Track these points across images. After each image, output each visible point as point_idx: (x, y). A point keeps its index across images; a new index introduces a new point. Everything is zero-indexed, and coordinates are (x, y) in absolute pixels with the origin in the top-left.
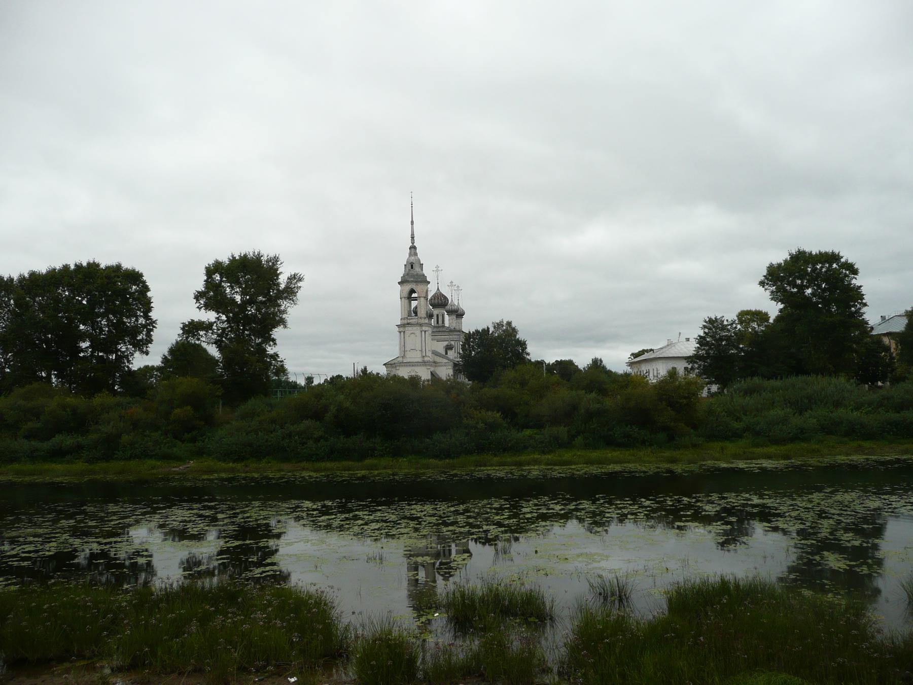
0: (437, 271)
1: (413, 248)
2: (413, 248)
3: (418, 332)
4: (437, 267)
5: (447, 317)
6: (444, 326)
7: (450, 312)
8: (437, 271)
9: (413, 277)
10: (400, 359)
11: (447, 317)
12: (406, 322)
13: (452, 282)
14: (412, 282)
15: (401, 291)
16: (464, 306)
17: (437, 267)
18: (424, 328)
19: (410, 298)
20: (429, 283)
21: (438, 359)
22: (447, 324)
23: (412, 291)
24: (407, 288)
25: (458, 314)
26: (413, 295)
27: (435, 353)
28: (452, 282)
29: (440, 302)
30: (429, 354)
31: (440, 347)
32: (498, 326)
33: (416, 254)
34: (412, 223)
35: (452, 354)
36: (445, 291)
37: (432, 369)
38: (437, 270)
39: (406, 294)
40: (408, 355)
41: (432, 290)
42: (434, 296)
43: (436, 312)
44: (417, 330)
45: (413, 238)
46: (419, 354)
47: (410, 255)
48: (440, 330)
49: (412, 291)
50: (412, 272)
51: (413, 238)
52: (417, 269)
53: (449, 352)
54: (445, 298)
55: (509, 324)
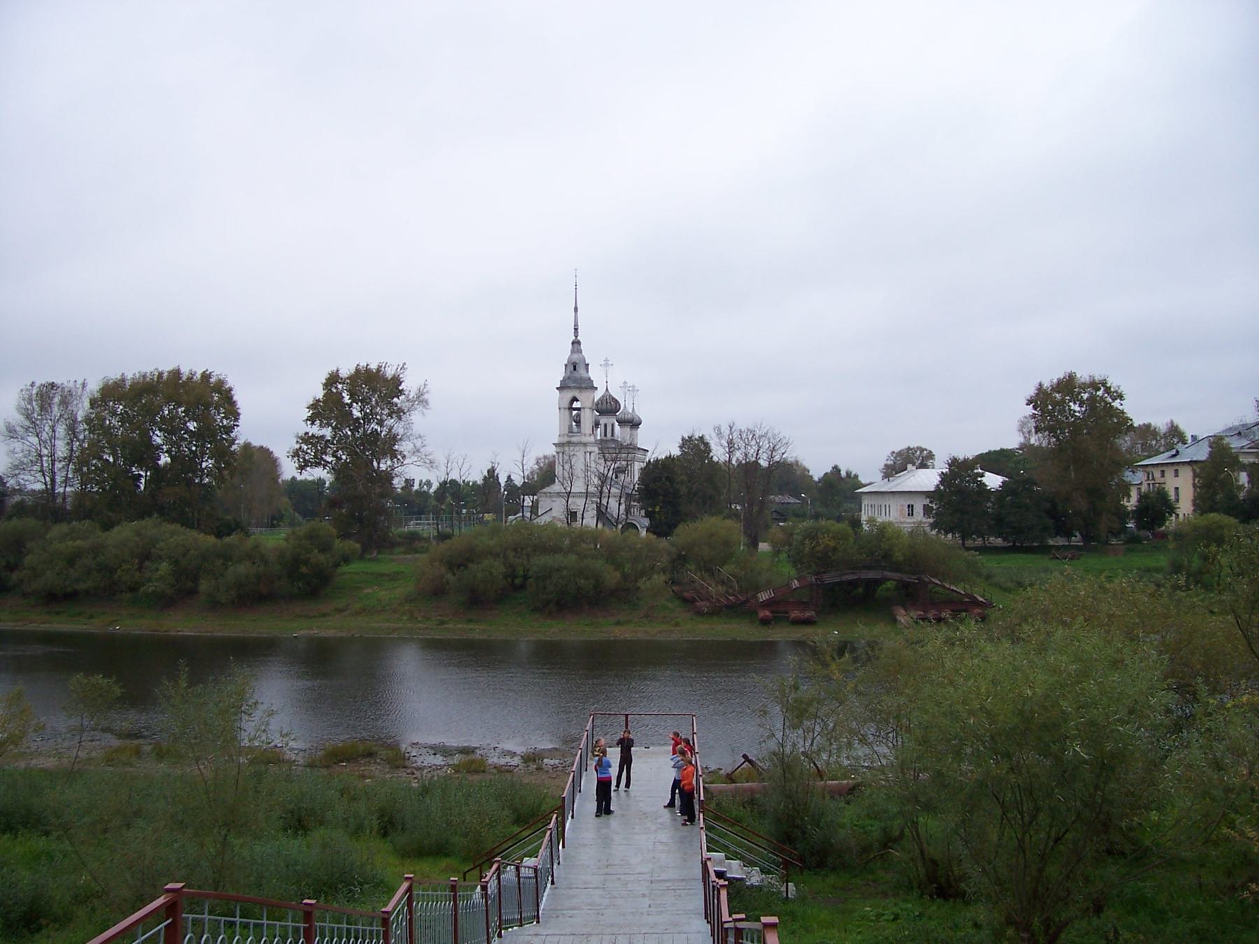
0: (606, 365)
1: (576, 343)
2: (576, 343)
4: (606, 360)
5: (617, 427)
7: (622, 423)
8: (606, 365)
11: (617, 427)
12: (566, 439)
15: (561, 399)
16: (641, 413)
17: (606, 360)
18: (589, 449)
19: (571, 409)
24: (569, 395)
25: (634, 424)
26: (576, 405)
29: (608, 407)
34: (576, 309)
39: (566, 404)
41: (598, 395)
42: (601, 400)
43: (603, 420)
47: (573, 352)
49: (575, 399)
50: (576, 374)
51: (576, 329)
52: (581, 372)
54: (616, 402)
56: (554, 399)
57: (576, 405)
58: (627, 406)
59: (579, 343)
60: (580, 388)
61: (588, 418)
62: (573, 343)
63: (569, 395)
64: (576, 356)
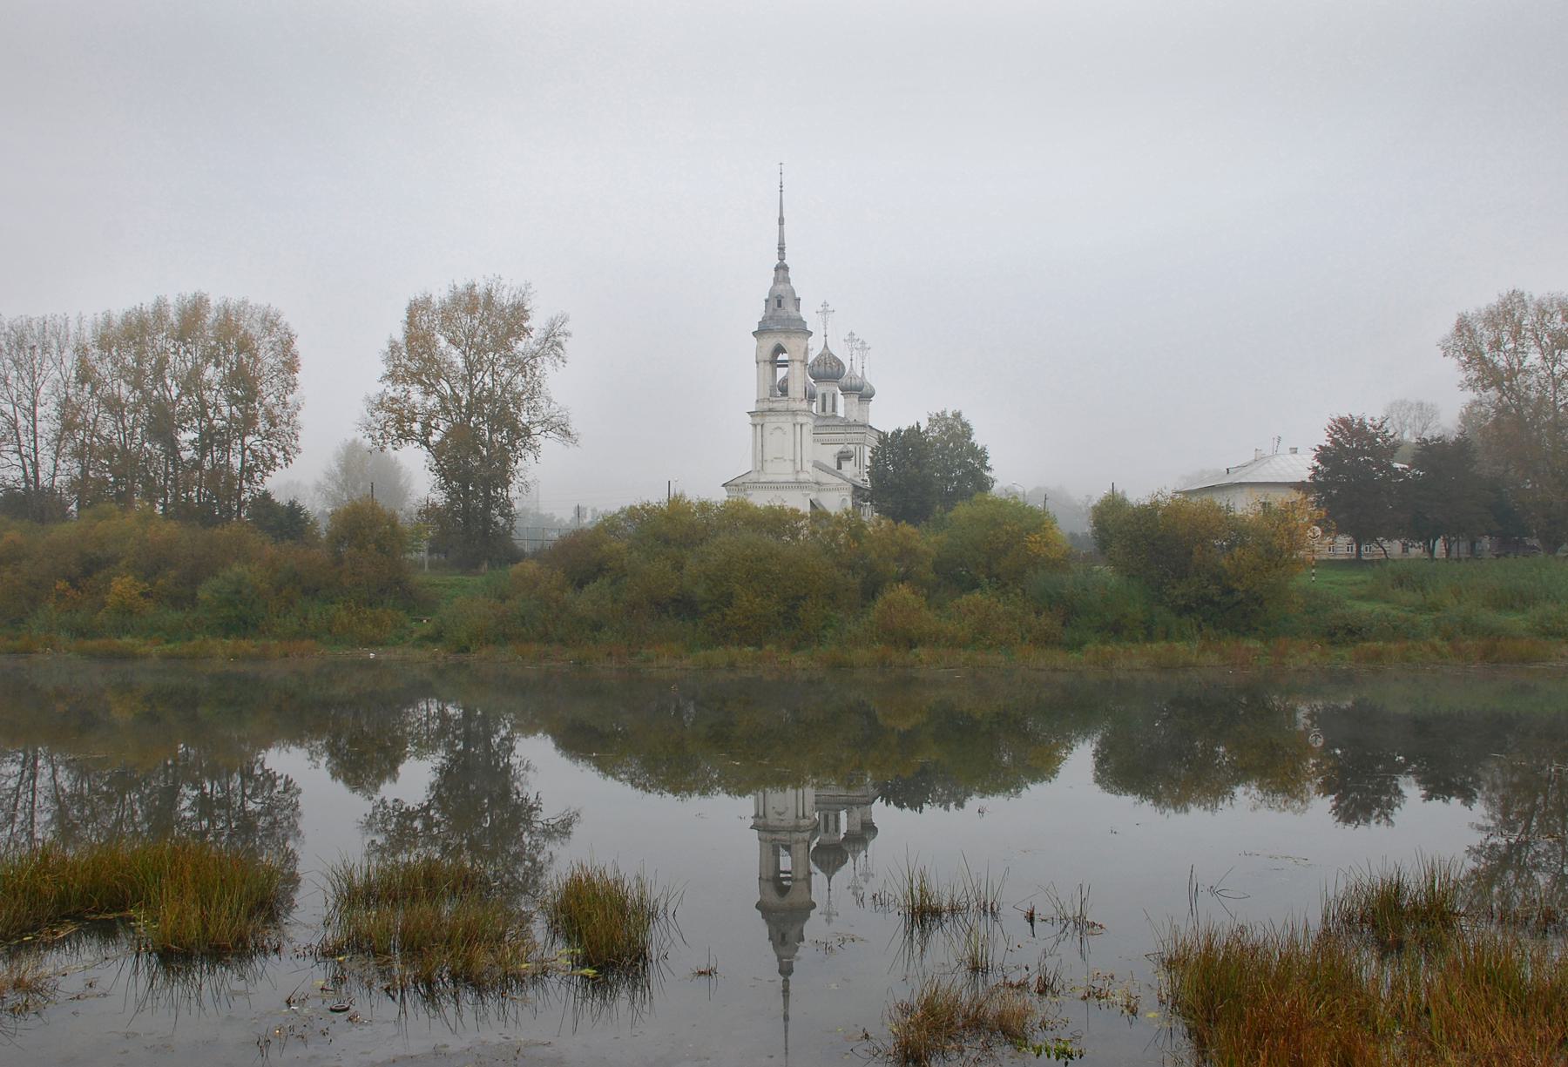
0: (825, 312)
1: (782, 269)
2: (782, 269)
3: (788, 427)
4: (825, 305)
5: (840, 399)
6: (835, 417)
7: (846, 390)
8: (825, 312)
9: (780, 319)
10: (754, 477)
11: (840, 399)
12: (766, 406)
13: (852, 334)
14: (780, 331)
15: (759, 348)
16: (872, 380)
17: (825, 305)
18: (800, 419)
19: (775, 363)
20: (811, 333)
21: (825, 478)
22: (841, 413)
23: (779, 349)
24: (770, 342)
25: (863, 394)
26: (781, 357)
27: (818, 465)
28: (852, 334)
29: (828, 371)
30: (808, 466)
31: (828, 455)
32: (937, 420)
33: (787, 280)
34: (781, 221)
35: (849, 468)
36: (840, 351)
37: (813, 496)
38: (825, 310)
39: (767, 355)
40: (769, 467)
41: (815, 348)
43: (820, 389)
44: (786, 422)
45: (781, 249)
46: (789, 467)
47: (776, 281)
48: (827, 423)
49: (779, 349)
50: (780, 312)
51: (781, 249)
52: (789, 308)
53: (844, 464)
54: (839, 363)
55: (957, 416)
56: (749, 349)
57: (781, 357)
58: (854, 365)
59: (786, 268)
60: (787, 332)
61: (798, 379)
62: (777, 269)
63: (770, 342)
64: (781, 287)
